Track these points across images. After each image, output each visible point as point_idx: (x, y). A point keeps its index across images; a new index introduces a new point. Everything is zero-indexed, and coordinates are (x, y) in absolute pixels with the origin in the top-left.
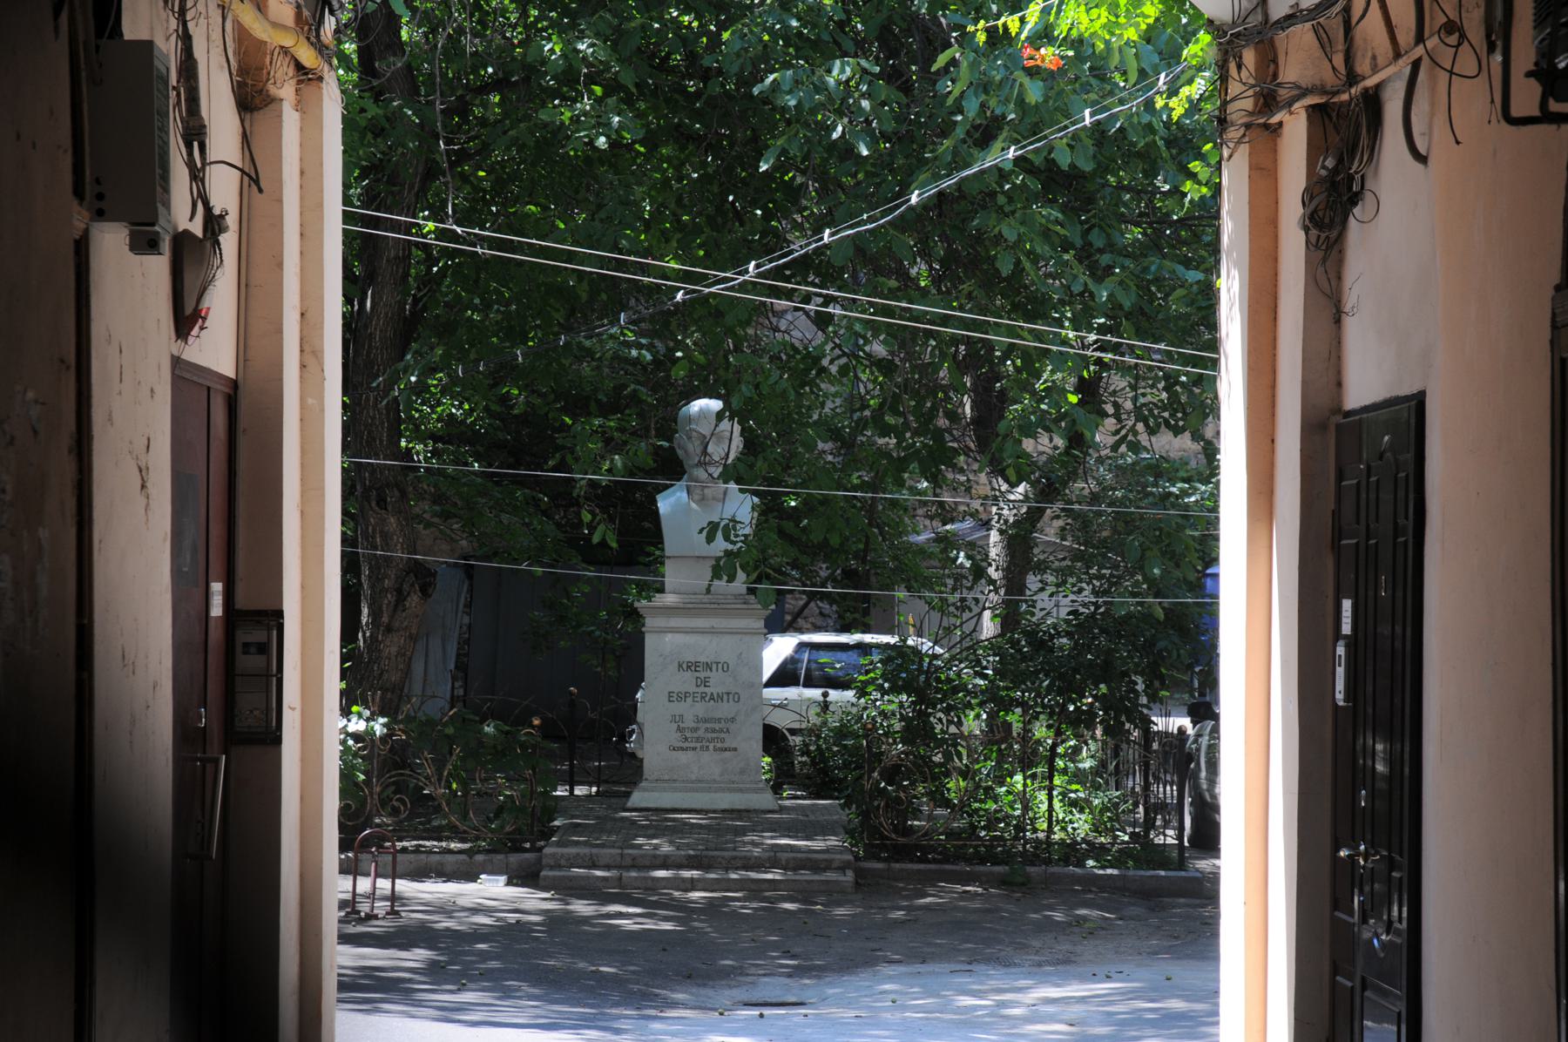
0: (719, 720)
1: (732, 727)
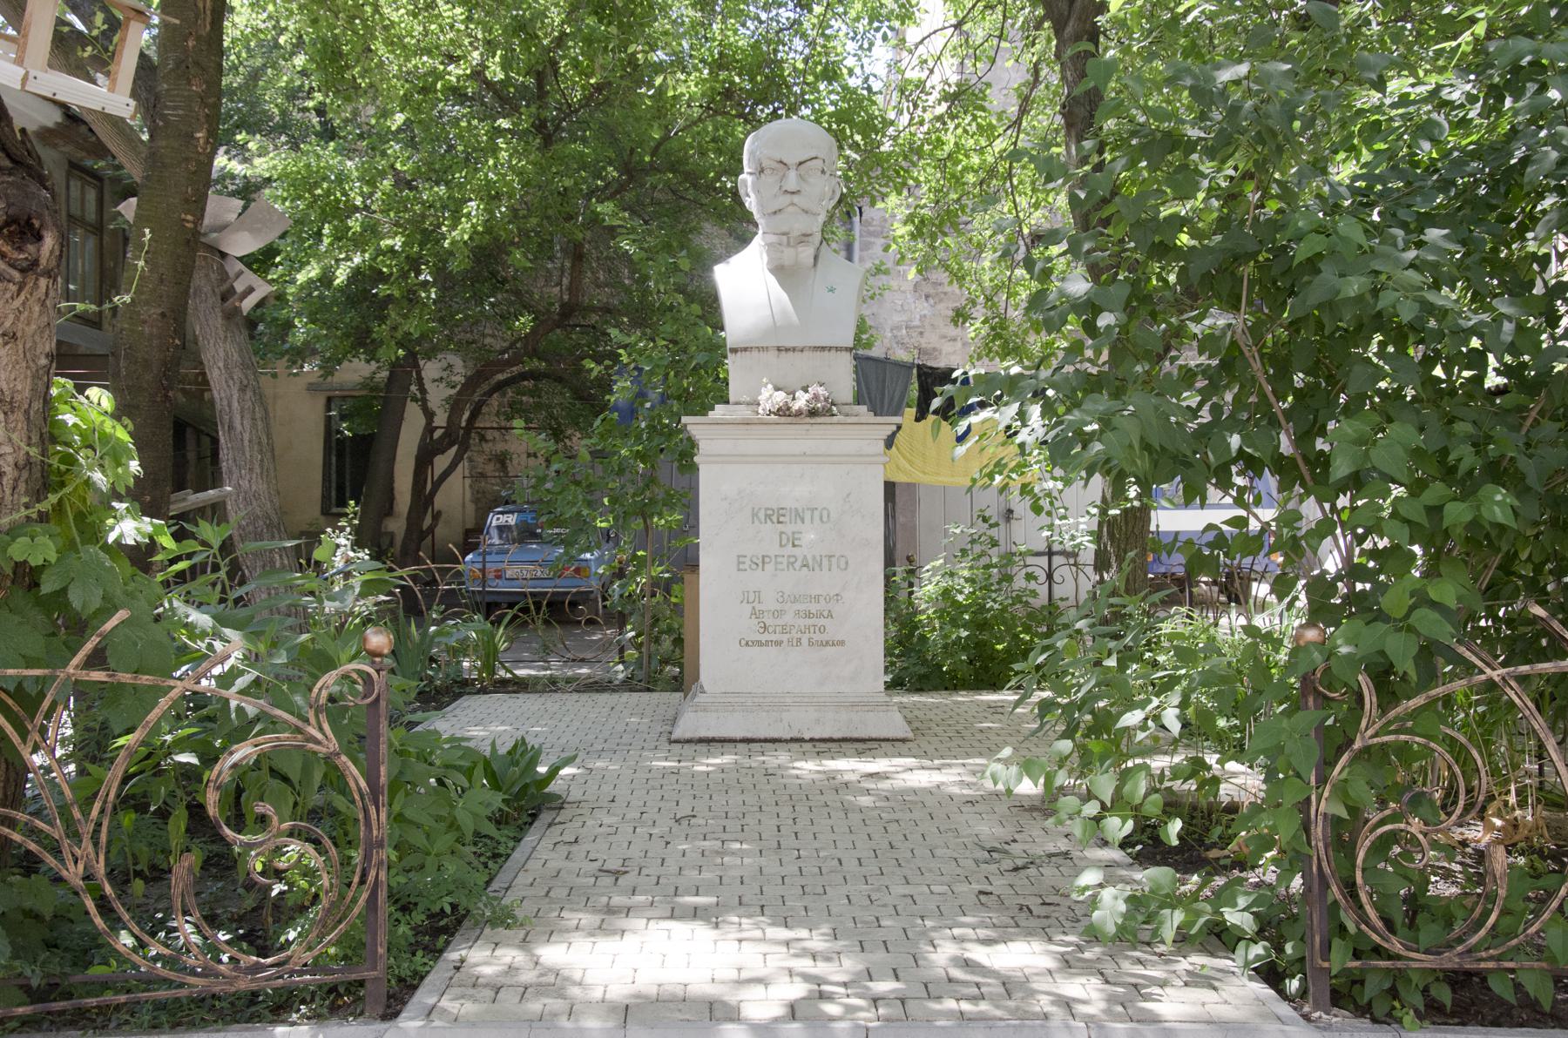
0: (817, 598)
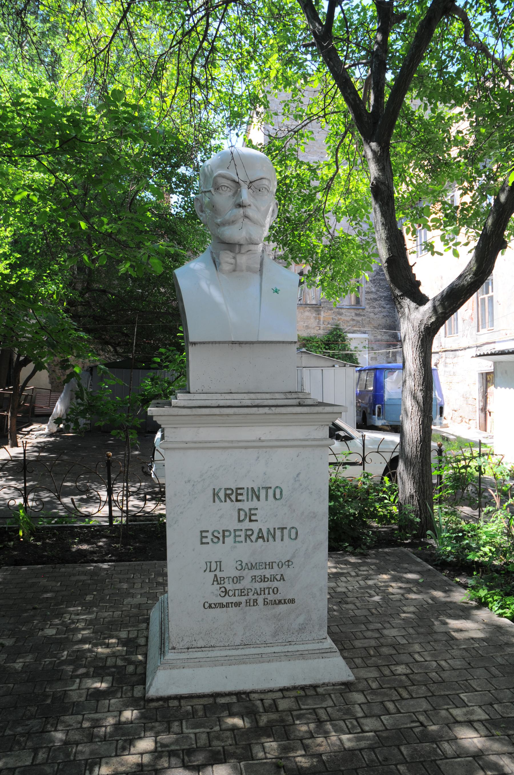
0: (271, 565)
1: (288, 572)
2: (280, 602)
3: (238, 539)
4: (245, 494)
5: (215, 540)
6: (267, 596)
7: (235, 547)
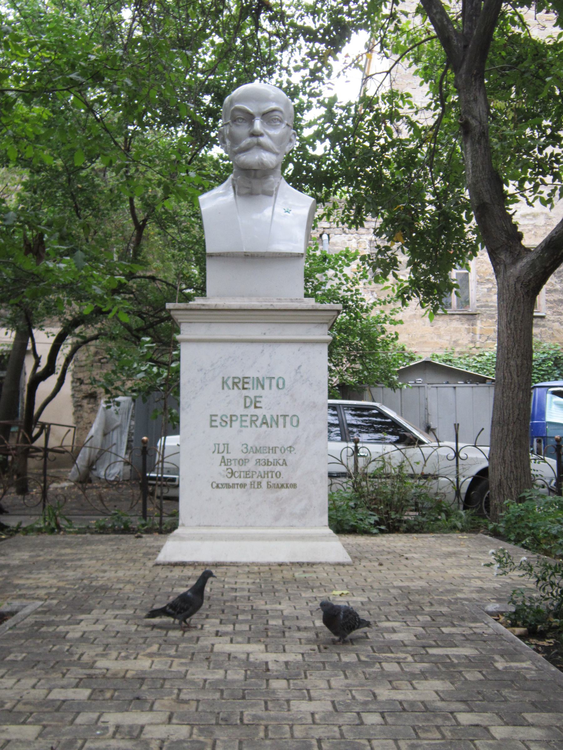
1: (290, 458)
2: (282, 486)
3: (244, 424)
4: (251, 382)
5: (224, 424)
6: (270, 479)
7: (241, 431)
